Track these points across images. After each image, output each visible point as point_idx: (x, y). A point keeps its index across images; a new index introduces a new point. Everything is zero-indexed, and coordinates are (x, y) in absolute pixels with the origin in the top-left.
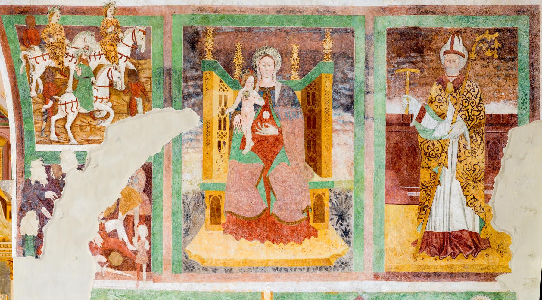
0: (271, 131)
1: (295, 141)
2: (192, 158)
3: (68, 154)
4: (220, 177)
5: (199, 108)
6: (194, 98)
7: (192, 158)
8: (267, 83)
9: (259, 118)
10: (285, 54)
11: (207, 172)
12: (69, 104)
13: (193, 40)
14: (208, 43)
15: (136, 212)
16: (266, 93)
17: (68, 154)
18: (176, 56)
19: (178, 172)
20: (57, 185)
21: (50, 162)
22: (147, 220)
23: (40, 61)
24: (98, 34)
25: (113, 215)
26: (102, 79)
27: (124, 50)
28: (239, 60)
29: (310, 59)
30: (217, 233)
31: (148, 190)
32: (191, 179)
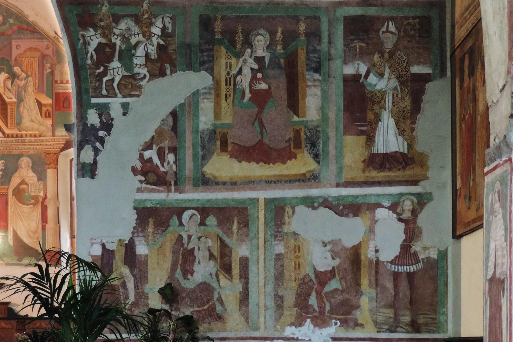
0: (263, 86)
1: (281, 94)
2: (207, 106)
3: (115, 104)
4: (227, 119)
5: (211, 71)
6: (208, 65)
7: (207, 106)
8: (260, 53)
9: (254, 78)
10: (273, 34)
11: (217, 115)
12: (116, 70)
13: (206, 23)
14: (218, 26)
15: (166, 144)
16: (259, 60)
17: (115, 104)
18: (194, 36)
19: (197, 115)
20: (107, 126)
21: (103, 110)
22: (173, 150)
23: (94, 40)
24: (138, 20)
25: (148, 146)
26: (140, 51)
27: (156, 30)
28: (239, 37)
29: (290, 37)
30: (225, 158)
31: (175, 128)
32: (206, 120)
